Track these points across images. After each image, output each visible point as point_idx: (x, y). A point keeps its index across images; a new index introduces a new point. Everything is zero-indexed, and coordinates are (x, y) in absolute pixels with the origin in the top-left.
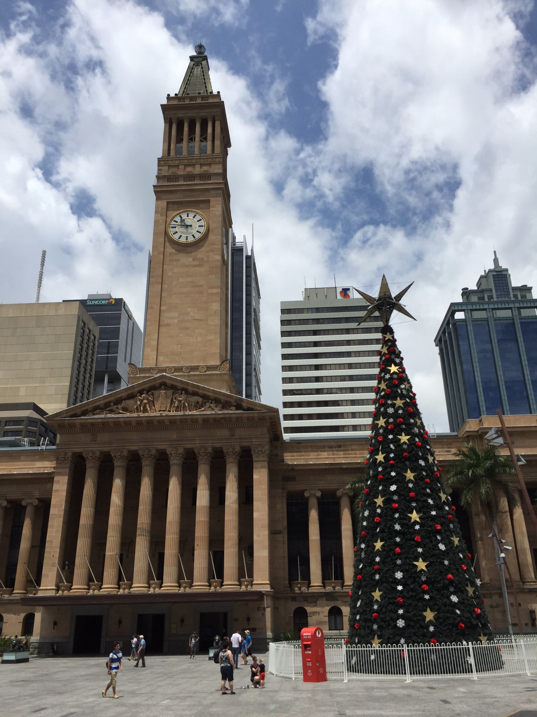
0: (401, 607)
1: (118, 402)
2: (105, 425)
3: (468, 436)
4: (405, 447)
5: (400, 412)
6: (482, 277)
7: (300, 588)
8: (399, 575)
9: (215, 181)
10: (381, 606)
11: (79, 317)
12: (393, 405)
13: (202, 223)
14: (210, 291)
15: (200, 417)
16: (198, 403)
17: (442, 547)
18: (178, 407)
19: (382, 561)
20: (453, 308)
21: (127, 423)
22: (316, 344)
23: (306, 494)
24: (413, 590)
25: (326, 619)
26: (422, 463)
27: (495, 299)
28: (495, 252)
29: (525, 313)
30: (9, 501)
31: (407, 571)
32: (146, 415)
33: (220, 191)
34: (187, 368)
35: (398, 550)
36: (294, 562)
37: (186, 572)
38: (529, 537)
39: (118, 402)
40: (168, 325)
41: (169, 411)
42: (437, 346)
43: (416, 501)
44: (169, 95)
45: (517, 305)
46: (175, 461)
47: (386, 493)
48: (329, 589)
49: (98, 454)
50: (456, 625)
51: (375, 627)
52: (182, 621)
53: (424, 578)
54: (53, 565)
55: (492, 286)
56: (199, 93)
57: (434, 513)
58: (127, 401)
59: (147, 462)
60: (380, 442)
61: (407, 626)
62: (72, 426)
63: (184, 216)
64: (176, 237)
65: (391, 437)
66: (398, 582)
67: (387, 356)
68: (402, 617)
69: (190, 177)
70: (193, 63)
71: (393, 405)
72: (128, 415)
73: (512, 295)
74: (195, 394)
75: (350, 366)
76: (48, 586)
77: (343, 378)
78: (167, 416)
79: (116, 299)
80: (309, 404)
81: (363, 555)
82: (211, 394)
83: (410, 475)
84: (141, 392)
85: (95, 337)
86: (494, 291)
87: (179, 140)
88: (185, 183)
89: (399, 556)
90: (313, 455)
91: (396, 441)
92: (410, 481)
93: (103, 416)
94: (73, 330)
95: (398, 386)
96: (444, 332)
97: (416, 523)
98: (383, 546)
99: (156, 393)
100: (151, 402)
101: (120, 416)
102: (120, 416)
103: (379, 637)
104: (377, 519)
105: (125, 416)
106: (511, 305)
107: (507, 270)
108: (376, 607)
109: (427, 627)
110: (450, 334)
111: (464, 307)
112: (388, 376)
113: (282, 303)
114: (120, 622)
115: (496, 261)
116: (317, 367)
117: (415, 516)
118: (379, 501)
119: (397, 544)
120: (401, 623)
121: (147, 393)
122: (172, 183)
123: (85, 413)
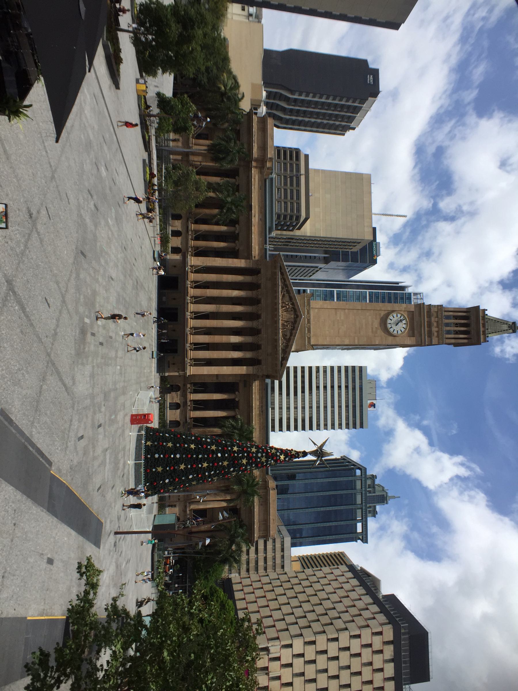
0: (164, 456)
2: (275, 285)
4: (240, 461)
5: (259, 460)
6: (383, 487)
7: (189, 388)
8: (178, 456)
9: (426, 340)
10: (165, 446)
11: (363, 240)
12: (262, 456)
13: (400, 332)
14: (356, 338)
16: (286, 336)
17: (191, 477)
19: (185, 448)
20: (363, 470)
21: (276, 298)
22: (340, 387)
23: (237, 393)
24: (171, 462)
25: (174, 402)
26: (232, 469)
27: (368, 495)
28: (399, 497)
29: (359, 512)
30: (238, 234)
31: (180, 460)
32: (280, 307)
33: (420, 343)
34: (310, 326)
35: (189, 456)
36: (202, 385)
37: (197, 331)
38: (213, 508)
40: (336, 313)
43: (213, 466)
44: (487, 310)
45: (364, 508)
47: (218, 451)
48: (189, 403)
49: (259, 282)
50: (155, 481)
51: (156, 443)
52: (174, 330)
53: (176, 467)
54: (203, 263)
55: (377, 494)
56: (487, 329)
57: (207, 474)
58: (288, 297)
60: (243, 449)
61: (155, 459)
62: (275, 268)
63: (404, 322)
64: (391, 317)
65: (246, 454)
66: (175, 456)
67: (290, 454)
68: (159, 457)
69: (430, 325)
70: (511, 324)
71: (262, 456)
72: (280, 298)
73: (370, 505)
74: (291, 334)
75: (325, 407)
76: (193, 261)
77: (318, 402)
78: (279, 319)
79: (376, 260)
80: (303, 382)
81: (189, 438)
82: (291, 343)
83: (226, 463)
84: (293, 304)
85: (351, 249)
86: (374, 494)
87: (456, 318)
88: (426, 322)
89: (187, 456)
90: (257, 397)
91: (243, 457)
92: (223, 463)
93: (280, 284)
94: (355, 237)
95: (272, 459)
96: (349, 462)
97: (202, 465)
98: (192, 448)
99: (292, 313)
101: (280, 293)
102: (280, 293)
103: (151, 445)
104: (205, 446)
105: (280, 295)
106: (364, 504)
107: (387, 503)
108: (164, 444)
109: (154, 468)
110: (347, 466)
111: (363, 476)
112: (278, 454)
113: (366, 367)
114: (174, 299)
115: (394, 497)
116: (325, 387)
117: (205, 465)
118: (214, 447)
119: (192, 455)
120: (157, 456)
121: (293, 308)
122: (426, 314)
123: (282, 274)
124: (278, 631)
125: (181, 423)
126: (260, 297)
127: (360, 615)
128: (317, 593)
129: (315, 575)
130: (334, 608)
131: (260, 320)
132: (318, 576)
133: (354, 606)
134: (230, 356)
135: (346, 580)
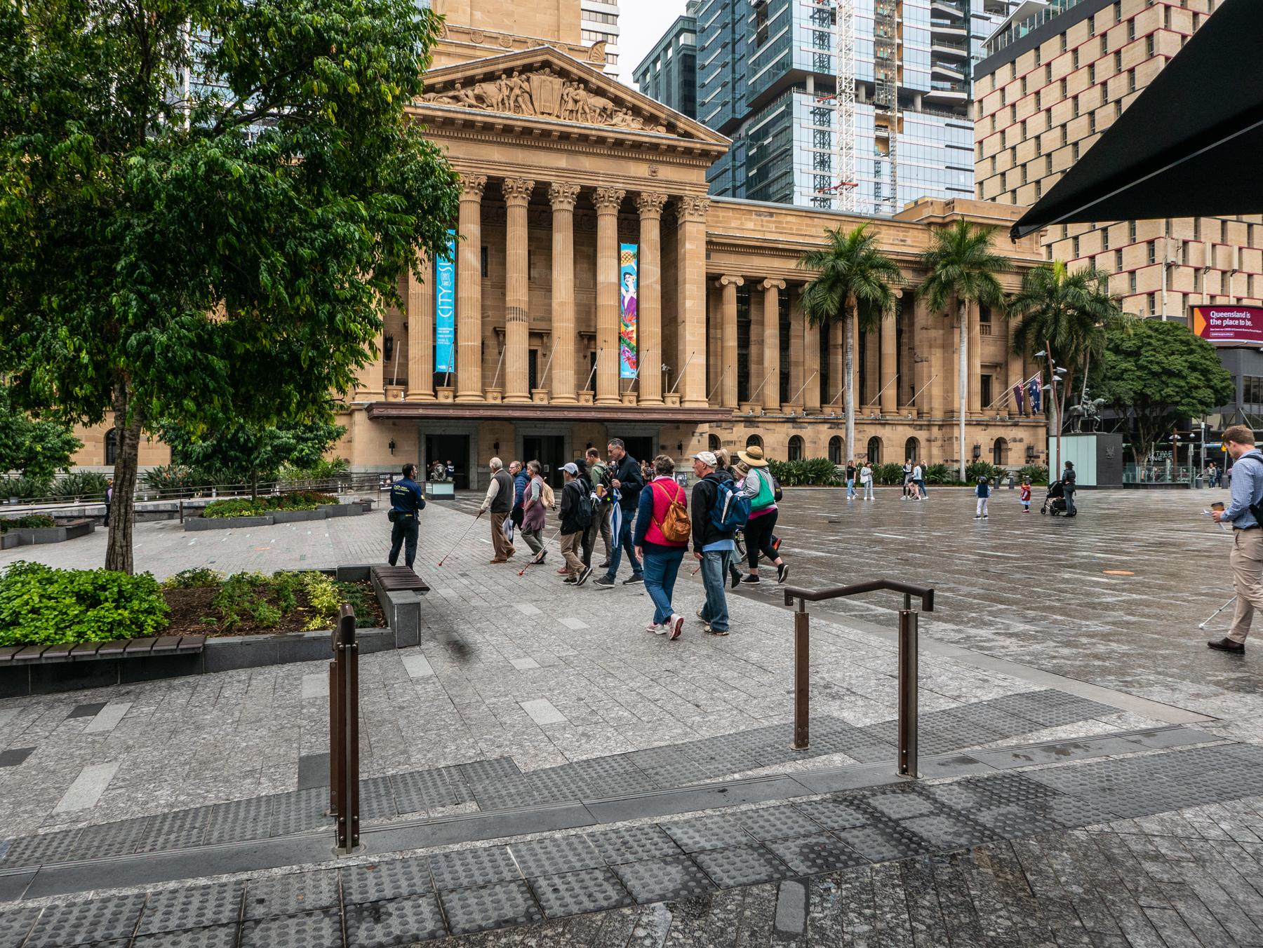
1: (469, 82)
3: (930, 224)
15: (611, 135)
16: (604, 109)
18: (572, 111)
20: (685, 25)
23: (724, 281)
39: (469, 82)
41: (558, 117)
42: (637, 81)
46: (566, 206)
59: (519, 202)
72: (489, 111)
82: (629, 98)
84: (509, 72)
99: (535, 78)
100: (526, 96)
102: (473, 110)
124: (1133, 241)
125: (793, 432)
126: (483, 180)
127: (1118, 53)
128: (1043, 152)
129: (993, 157)
130: (1092, 114)
131: (555, 186)
132: (998, 148)
133: (1091, 66)
134: (658, 287)
135: (1018, 83)
